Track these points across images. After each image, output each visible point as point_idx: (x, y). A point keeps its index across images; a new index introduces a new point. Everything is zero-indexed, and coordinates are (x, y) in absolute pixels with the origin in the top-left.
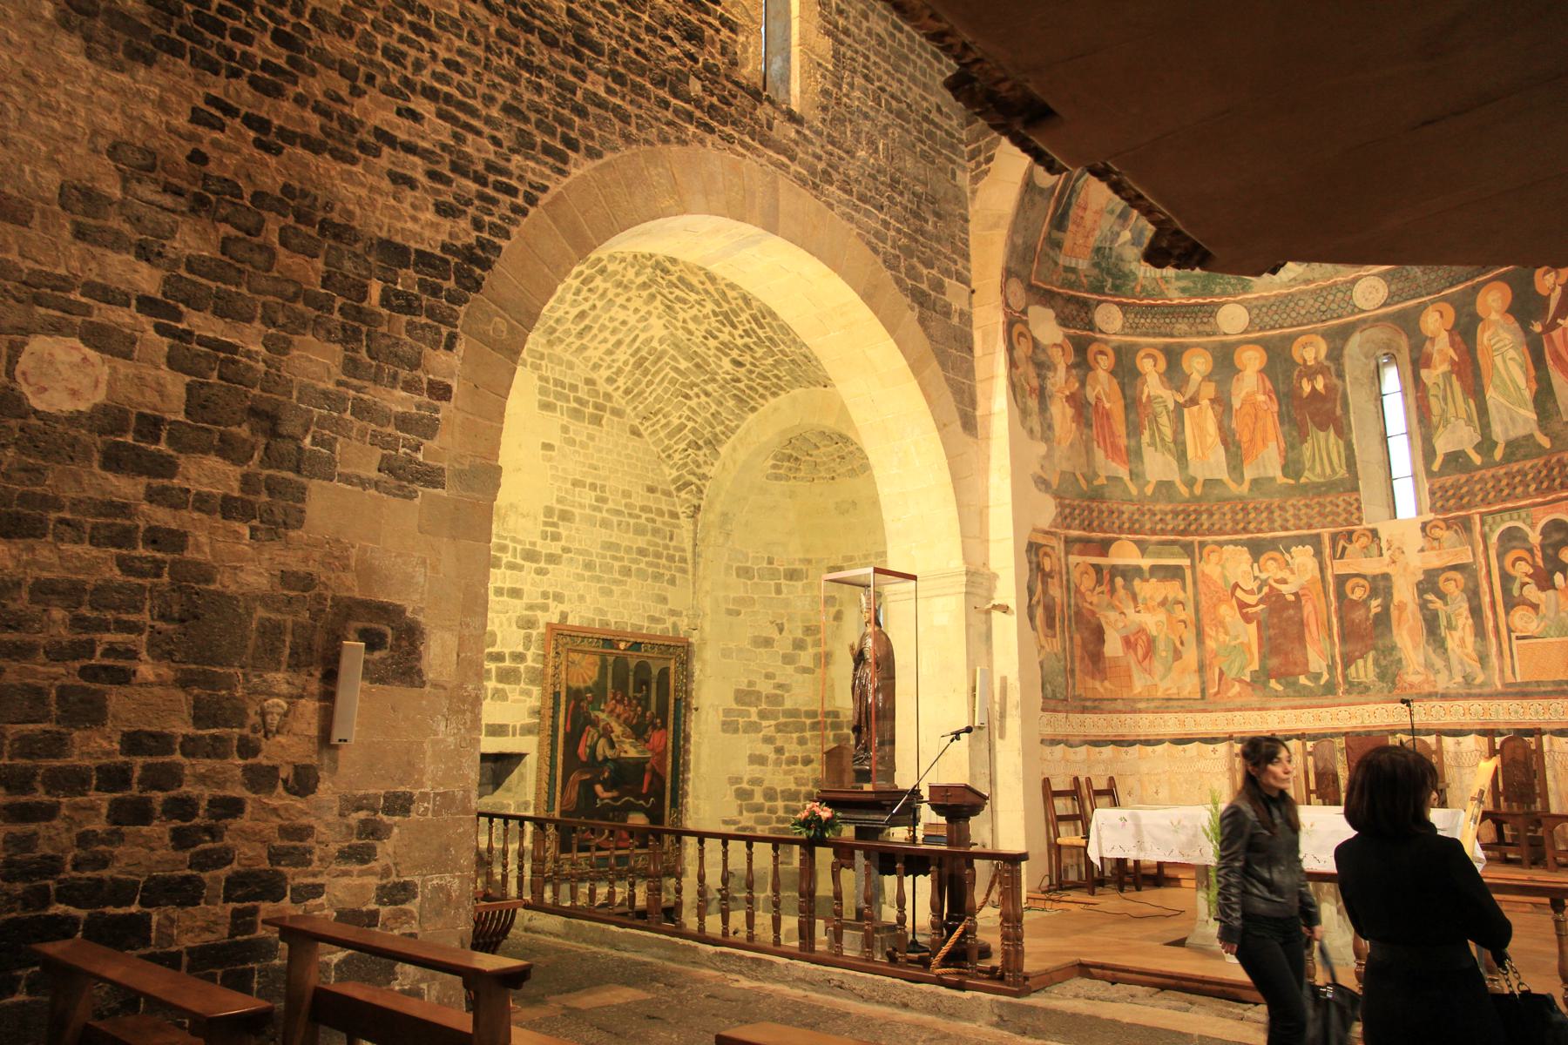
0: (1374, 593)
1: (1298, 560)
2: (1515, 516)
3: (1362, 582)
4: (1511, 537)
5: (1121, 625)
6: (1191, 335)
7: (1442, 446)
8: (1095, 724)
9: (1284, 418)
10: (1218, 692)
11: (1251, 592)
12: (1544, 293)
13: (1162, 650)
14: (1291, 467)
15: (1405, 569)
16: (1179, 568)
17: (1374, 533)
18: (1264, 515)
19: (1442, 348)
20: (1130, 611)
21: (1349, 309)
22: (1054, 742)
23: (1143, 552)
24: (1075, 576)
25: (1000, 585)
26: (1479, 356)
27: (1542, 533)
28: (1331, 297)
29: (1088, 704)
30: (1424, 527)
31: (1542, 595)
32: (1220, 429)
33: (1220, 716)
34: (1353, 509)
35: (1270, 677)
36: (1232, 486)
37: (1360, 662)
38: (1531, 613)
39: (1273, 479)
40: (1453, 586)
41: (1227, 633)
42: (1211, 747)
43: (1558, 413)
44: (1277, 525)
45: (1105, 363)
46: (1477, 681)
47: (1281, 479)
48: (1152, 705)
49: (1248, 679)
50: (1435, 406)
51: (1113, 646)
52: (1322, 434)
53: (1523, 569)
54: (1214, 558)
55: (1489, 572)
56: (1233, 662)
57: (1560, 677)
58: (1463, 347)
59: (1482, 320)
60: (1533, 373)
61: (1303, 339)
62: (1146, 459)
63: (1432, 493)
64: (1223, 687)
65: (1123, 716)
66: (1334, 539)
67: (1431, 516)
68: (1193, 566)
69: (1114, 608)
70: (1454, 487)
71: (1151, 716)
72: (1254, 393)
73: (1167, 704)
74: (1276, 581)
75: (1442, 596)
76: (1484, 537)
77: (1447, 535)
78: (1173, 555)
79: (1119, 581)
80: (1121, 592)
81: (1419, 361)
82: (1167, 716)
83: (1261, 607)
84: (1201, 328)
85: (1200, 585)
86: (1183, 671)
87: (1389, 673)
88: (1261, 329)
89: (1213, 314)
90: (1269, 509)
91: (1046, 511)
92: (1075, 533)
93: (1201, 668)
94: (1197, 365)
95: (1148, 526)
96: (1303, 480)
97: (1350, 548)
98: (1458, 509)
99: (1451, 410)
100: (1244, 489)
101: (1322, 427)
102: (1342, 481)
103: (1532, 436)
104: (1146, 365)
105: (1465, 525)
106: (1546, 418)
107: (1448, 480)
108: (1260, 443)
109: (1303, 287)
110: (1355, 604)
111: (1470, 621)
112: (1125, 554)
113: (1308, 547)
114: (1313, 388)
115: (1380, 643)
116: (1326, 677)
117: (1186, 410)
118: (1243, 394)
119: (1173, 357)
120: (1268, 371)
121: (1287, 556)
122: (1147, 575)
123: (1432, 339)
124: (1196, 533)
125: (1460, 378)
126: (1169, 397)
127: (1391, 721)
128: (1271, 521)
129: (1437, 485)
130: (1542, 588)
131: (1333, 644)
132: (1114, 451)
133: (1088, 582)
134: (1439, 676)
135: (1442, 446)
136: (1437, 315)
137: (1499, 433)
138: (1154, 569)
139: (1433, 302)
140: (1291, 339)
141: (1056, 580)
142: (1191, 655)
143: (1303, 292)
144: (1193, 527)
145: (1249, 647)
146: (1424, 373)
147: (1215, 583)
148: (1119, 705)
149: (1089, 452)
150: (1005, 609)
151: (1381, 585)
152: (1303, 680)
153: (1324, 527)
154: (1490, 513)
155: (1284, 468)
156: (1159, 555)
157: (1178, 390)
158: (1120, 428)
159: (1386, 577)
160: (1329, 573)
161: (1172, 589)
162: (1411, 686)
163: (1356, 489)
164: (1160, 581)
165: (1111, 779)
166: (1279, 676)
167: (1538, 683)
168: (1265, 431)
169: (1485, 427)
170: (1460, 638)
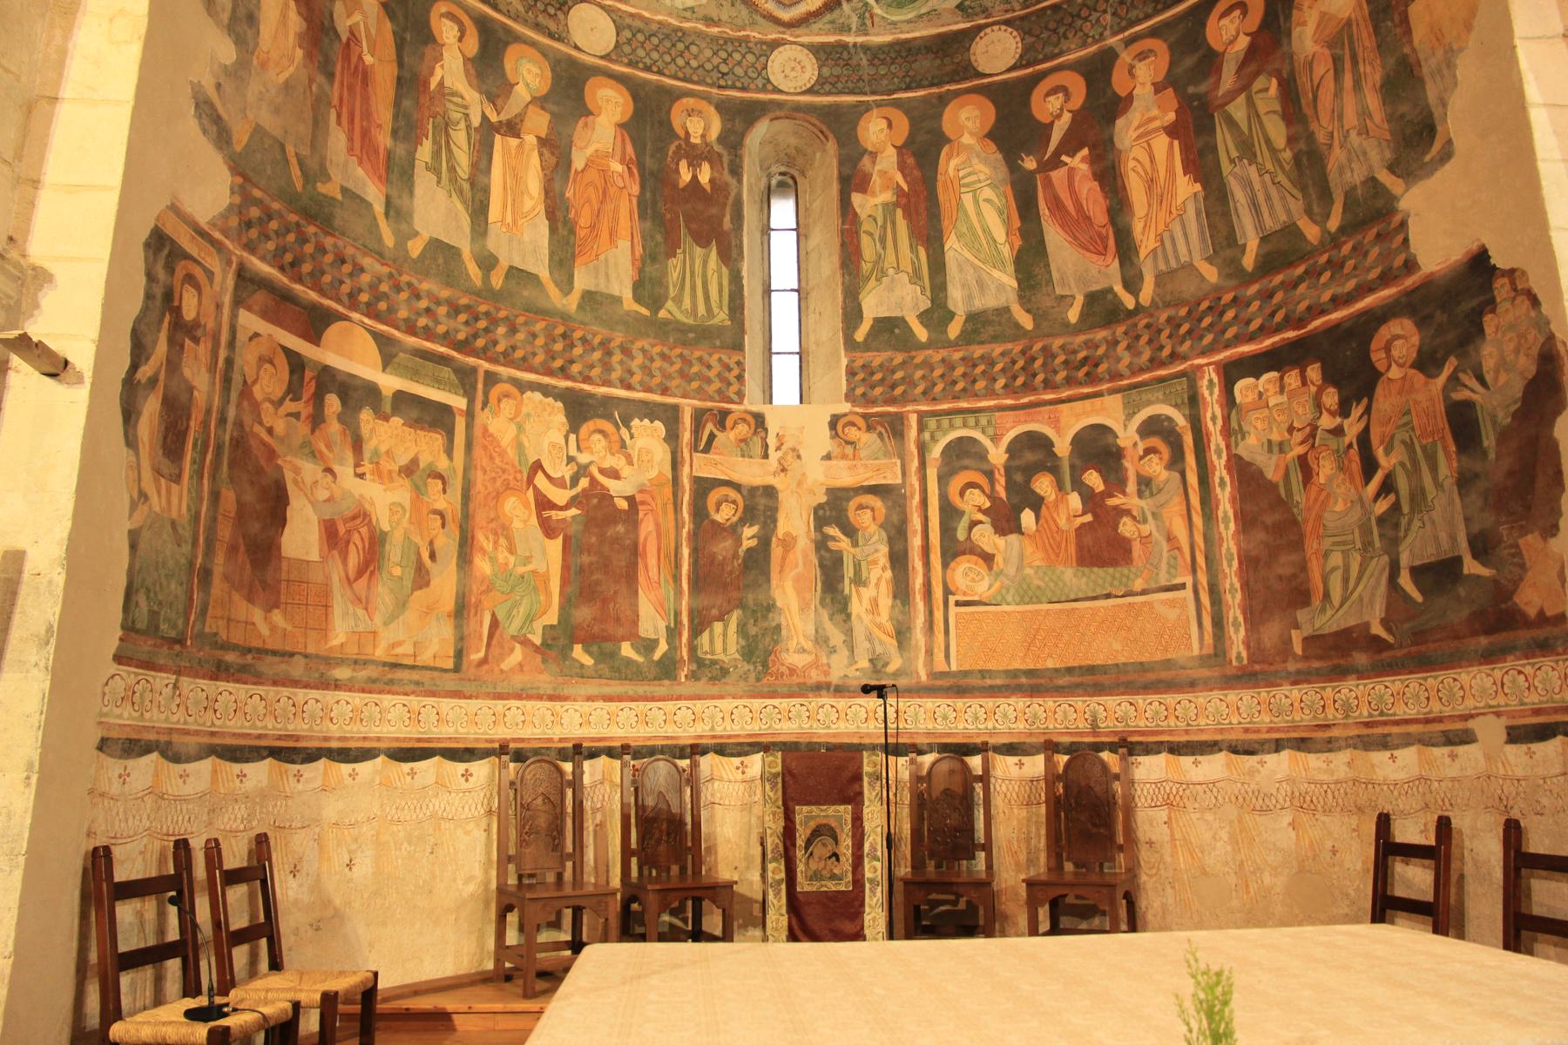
0: (749, 515)
1: (640, 443)
2: (971, 421)
3: (733, 494)
4: (962, 453)
5: (322, 495)
6: (525, 22)
7: (874, 305)
8: (243, 708)
9: (646, 208)
10: (484, 661)
11: (558, 483)
12: (1045, 119)
13: (396, 563)
14: (649, 288)
15: (799, 484)
16: (446, 410)
17: (759, 421)
18: (597, 355)
19: (886, 167)
20: (345, 471)
21: (760, 82)
22: (133, 747)
23: (387, 362)
24: (247, 358)
25: (49, 300)
26: (940, 190)
27: (1008, 450)
28: (737, 57)
29: (230, 657)
30: (834, 423)
31: (1001, 541)
32: (548, 191)
33: (481, 707)
34: (731, 376)
35: (574, 640)
36: (553, 291)
37: (718, 627)
38: (981, 567)
39: (617, 300)
40: (868, 517)
41: (512, 550)
42: (461, 767)
43: (1050, 281)
44: (615, 376)
46: (891, 668)
47: (629, 304)
48: (363, 674)
49: (537, 640)
50: (868, 247)
51: (301, 537)
52: (698, 251)
53: (976, 498)
54: (507, 407)
55: (924, 502)
56: (516, 605)
57: (1017, 665)
58: (917, 173)
59: (948, 141)
60: (1017, 223)
61: (689, 102)
62: (419, 190)
63: (851, 373)
64: (495, 651)
65: (301, 694)
66: (699, 417)
67: (846, 407)
68: (470, 414)
69: (314, 455)
71: (357, 699)
72: (607, 156)
73: (392, 675)
74: (602, 471)
75: (850, 531)
76: (922, 449)
77: (868, 440)
78: (438, 383)
79: (333, 403)
80: (334, 427)
81: (852, 180)
82: (387, 700)
83: (574, 511)
84: (541, 19)
85: (478, 452)
86: (429, 611)
87: (760, 649)
88: (630, 64)
90: (605, 345)
91: (209, 194)
92: (265, 269)
93: (461, 610)
94: (528, 75)
95: (403, 313)
96: (662, 314)
97: (720, 436)
98: (891, 401)
99: (890, 258)
100: (571, 303)
101: (703, 241)
102: (720, 330)
103: (1007, 309)
104: (447, 32)
105: (895, 427)
106: (1032, 287)
107: (878, 358)
108: (605, 235)
109: (701, 27)
110: (718, 528)
111: (889, 574)
112: (351, 352)
113: (658, 424)
114: (695, 177)
115: (750, 598)
116: (663, 647)
117: (498, 137)
118: (590, 151)
120: (632, 128)
121: (624, 432)
122: (387, 408)
123: (874, 155)
124: (483, 353)
125: (908, 215)
126: (475, 104)
127: (755, 728)
128: (607, 368)
129: (860, 362)
130: (1001, 530)
131: (679, 592)
132: (363, 146)
133: (270, 384)
134: (834, 657)
135: (874, 305)
136: (883, 124)
137: (956, 298)
138: (401, 398)
139: (879, 105)
140: (674, 96)
141: (203, 349)
142: (445, 581)
143: (700, 34)
144: (480, 343)
145: (546, 579)
146: (856, 198)
147: (503, 454)
148: (297, 669)
149: (318, 123)
150: (57, 368)
151: (760, 505)
152: (627, 650)
153: (684, 397)
154: (934, 414)
155: (638, 287)
156: (415, 375)
157: (492, 98)
158: (384, 114)
159: (770, 492)
160: (686, 470)
161: (427, 447)
162: (792, 671)
163: (739, 347)
164: (415, 424)
165: (262, 841)
167: (983, 673)
168: (616, 220)
169: (938, 288)
170: (871, 599)
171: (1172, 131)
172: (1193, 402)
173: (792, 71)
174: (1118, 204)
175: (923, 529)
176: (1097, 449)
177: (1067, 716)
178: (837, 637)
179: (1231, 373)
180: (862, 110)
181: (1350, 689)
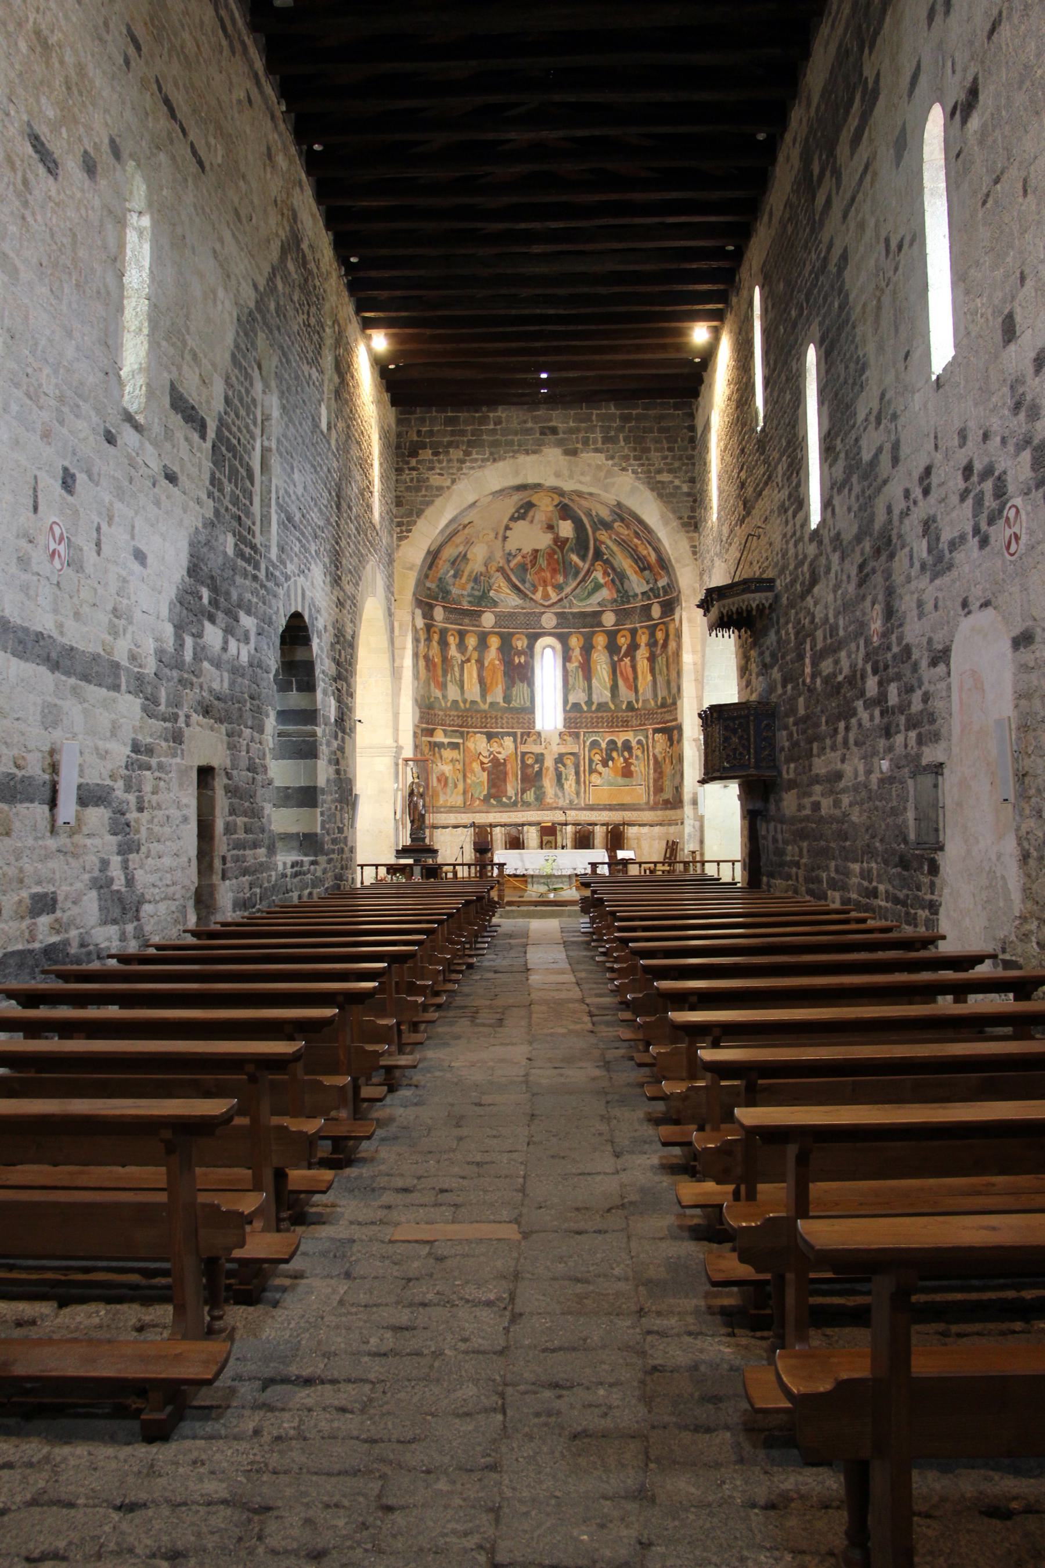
0: (536, 761)
4: (595, 744)
9: (506, 674)
13: (450, 784)
14: (507, 698)
19: (576, 653)
23: (446, 735)
40: (569, 761)
45: (436, 637)
47: (502, 704)
50: (571, 680)
53: (597, 757)
66: (522, 734)
70: (576, 717)
73: (452, 809)
75: (564, 765)
77: (569, 739)
87: (540, 798)
89: (480, 616)
93: (465, 793)
94: (472, 641)
100: (486, 707)
101: (522, 681)
105: (577, 736)
107: (572, 715)
119: (462, 635)
120: (500, 649)
133: (426, 750)
135: (572, 699)
137: (595, 698)
140: (513, 634)
151: (540, 758)
158: (440, 672)
159: (542, 754)
163: (533, 713)
166: (494, 797)
169: (590, 695)
170: (570, 784)
171: (648, 659)
172: (647, 737)
173: (549, 620)
174: (636, 678)
175: (584, 766)
176: (627, 746)
177: (616, 817)
178: (560, 794)
179: (656, 731)
180: (570, 633)
181: (668, 812)
